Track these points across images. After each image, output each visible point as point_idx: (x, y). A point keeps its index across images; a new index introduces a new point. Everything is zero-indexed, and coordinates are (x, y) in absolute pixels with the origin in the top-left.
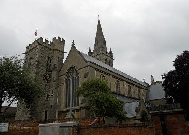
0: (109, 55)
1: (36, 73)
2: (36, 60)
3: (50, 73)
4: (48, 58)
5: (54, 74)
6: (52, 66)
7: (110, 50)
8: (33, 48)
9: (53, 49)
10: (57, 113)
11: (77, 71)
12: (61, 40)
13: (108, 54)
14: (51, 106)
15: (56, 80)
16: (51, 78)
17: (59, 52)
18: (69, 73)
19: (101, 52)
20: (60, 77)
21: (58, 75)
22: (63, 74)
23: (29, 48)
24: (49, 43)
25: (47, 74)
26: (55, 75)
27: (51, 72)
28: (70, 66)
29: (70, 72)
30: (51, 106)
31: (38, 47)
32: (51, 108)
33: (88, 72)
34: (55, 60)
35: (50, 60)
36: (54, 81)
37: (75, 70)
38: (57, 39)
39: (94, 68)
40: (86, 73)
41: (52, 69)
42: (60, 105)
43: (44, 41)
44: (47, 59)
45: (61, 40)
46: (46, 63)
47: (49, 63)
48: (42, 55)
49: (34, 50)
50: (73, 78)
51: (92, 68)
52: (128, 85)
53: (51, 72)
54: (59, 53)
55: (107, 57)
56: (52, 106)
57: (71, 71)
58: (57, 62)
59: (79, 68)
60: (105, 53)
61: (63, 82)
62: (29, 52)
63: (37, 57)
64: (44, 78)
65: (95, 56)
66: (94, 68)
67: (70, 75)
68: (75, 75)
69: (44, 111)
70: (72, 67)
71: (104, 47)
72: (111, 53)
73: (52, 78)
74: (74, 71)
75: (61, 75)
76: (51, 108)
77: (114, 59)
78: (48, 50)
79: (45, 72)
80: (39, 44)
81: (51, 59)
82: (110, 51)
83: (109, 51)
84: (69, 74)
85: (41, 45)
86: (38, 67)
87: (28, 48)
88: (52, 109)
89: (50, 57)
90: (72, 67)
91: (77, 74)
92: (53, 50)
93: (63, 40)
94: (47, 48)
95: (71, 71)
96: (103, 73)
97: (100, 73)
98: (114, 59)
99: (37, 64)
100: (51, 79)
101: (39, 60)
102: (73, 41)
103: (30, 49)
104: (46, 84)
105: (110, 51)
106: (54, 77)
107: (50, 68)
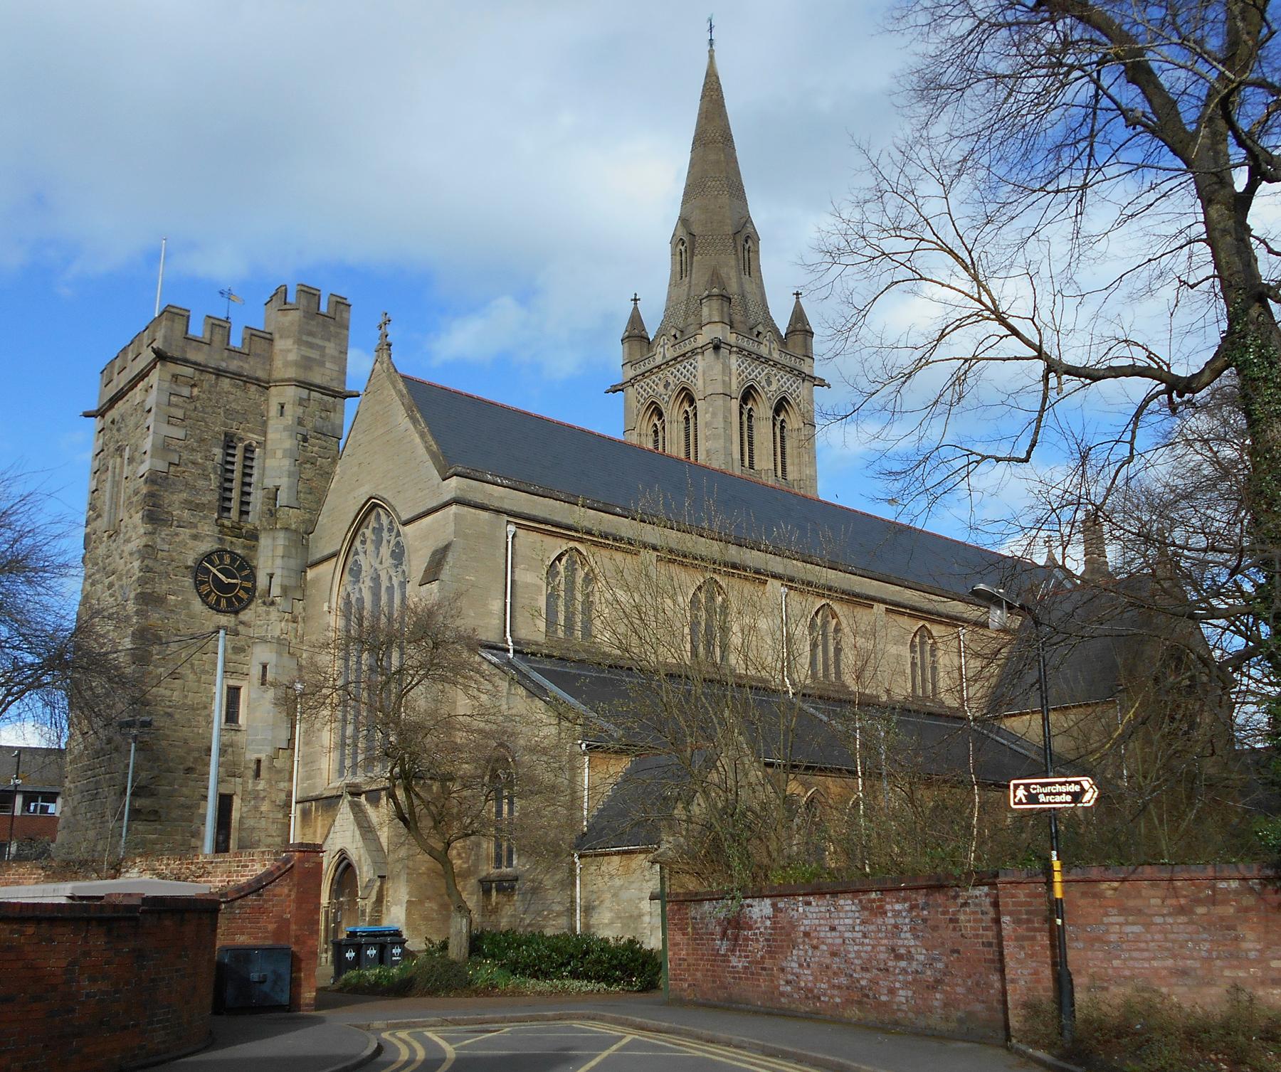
0: (776, 355)
1: (148, 552)
2: (144, 468)
3: (245, 547)
4: (229, 443)
5: (271, 559)
6: (257, 498)
8: (133, 384)
9: (260, 374)
10: (296, 810)
11: (398, 534)
12: (324, 308)
13: (766, 348)
15: (285, 590)
16: (252, 577)
17: (304, 393)
18: (357, 543)
19: (702, 339)
20: (311, 574)
22: (327, 552)
23: (115, 382)
24: (236, 342)
25: (221, 559)
26: (279, 562)
27: (256, 538)
28: (362, 495)
29: (363, 542)
30: (259, 761)
31: (154, 377)
32: (257, 774)
33: (446, 548)
34: (279, 454)
35: (239, 452)
36: (273, 603)
37: (390, 530)
38: (291, 298)
39: (498, 511)
40: (434, 554)
41: (253, 519)
42: (309, 761)
43: (197, 329)
44: (218, 452)
46: (214, 482)
47: (237, 468)
48: (180, 433)
49: (137, 395)
50: (376, 579)
51: (485, 515)
53: (253, 536)
55: (759, 374)
56: (263, 765)
57: (368, 532)
58: (286, 463)
59: (405, 517)
60: (745, 344)
61: (326, 608)
62: (113, 401)
63: (148, 444)
64: (203, 583)
65: (667, 363)
66: (498, 511)
67: (361, 557)
68: (388, 561)
70: (371, 507)
71: (733, 288)
72: (800, 327)
73: (262, 581)
74: (385, 534)
75: (318, 556)
77: (822, 383)
78: (226, 383)
79: (206, 546)
80: (161, 356)
81: (249, 449)
82: (799, 316)
84: (356, 553)
85: (174, 360)
86: (155, 516)
87: (107, 372)
88: (262, 785)
89: (241, 440)
90: (376, 505)
91: (398, 554)
92: (264, 385)
93: (341, 304)
94: (219, 373)
95: (368, 532)
96: (580, 540)
97: (549, 540)
98: (822, 383)
99: (151, 495)
100: (251, 591)
101: (161, 466)
103: (121, 381)
104: (223, 620)
105: (799, 316)
106: (271, 576)
107: (244, 513)
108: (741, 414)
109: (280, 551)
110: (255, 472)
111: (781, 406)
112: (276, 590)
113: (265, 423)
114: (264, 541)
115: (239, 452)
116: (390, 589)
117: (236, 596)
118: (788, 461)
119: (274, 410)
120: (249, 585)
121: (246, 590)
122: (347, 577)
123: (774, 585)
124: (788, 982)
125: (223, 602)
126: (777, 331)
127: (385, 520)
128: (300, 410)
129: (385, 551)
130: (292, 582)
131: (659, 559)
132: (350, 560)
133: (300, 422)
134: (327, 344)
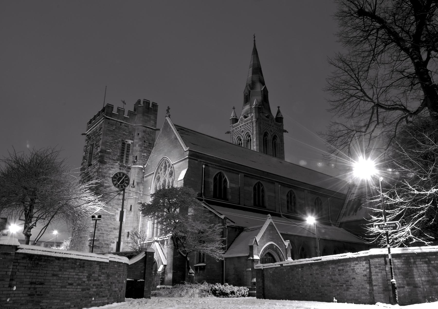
7: (279, 112)
11: (171, 168)
12: (151, 106)
14: (128, 233)
15: (138, 183)
18: (159, 170)
21: (141, 176)
26: (136, 175)
27: (130, 169)
29: (161, 170)
32: (128, 236)
34: (137, 145)
36: (134, 187)
44: (120, 145)
45: (151, 106)
50: (165, 181)
52: (287, 190)
54: (144, 132)
64: (115, 181)
67: (160, 174)
69: (114, 243)
76: (128, 236)
77: (286, 131)
83: (274, 114)
84: (159, 173)
96: (223, 170)
98: (286, 131)
99: (101, 156)
102: (169, 108)
108: (264, 139)
109: (137, 173)
110: (131, 151)
111: (275, 138)
112: (135, 184)
113: (133, 137)
114: (132, 170)
115: (126, 146)
116: (169, 182)
117: (124, 185)
118: (277, 152)
119: (136, 134)
120: (128, 182)
121: (127, 183)
122: (156, 179)
123: (276, 184)
124: (296, 292)
125: (120, 186)
126: (273, 118)
127: (168, 164)
128: (143, 134)
129: (167, 172)
130: (140, 181)
131: (245, 176)
132: (157, 175)
133: (143, 137)
134: (151, 116)
